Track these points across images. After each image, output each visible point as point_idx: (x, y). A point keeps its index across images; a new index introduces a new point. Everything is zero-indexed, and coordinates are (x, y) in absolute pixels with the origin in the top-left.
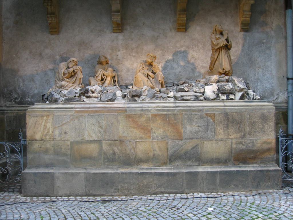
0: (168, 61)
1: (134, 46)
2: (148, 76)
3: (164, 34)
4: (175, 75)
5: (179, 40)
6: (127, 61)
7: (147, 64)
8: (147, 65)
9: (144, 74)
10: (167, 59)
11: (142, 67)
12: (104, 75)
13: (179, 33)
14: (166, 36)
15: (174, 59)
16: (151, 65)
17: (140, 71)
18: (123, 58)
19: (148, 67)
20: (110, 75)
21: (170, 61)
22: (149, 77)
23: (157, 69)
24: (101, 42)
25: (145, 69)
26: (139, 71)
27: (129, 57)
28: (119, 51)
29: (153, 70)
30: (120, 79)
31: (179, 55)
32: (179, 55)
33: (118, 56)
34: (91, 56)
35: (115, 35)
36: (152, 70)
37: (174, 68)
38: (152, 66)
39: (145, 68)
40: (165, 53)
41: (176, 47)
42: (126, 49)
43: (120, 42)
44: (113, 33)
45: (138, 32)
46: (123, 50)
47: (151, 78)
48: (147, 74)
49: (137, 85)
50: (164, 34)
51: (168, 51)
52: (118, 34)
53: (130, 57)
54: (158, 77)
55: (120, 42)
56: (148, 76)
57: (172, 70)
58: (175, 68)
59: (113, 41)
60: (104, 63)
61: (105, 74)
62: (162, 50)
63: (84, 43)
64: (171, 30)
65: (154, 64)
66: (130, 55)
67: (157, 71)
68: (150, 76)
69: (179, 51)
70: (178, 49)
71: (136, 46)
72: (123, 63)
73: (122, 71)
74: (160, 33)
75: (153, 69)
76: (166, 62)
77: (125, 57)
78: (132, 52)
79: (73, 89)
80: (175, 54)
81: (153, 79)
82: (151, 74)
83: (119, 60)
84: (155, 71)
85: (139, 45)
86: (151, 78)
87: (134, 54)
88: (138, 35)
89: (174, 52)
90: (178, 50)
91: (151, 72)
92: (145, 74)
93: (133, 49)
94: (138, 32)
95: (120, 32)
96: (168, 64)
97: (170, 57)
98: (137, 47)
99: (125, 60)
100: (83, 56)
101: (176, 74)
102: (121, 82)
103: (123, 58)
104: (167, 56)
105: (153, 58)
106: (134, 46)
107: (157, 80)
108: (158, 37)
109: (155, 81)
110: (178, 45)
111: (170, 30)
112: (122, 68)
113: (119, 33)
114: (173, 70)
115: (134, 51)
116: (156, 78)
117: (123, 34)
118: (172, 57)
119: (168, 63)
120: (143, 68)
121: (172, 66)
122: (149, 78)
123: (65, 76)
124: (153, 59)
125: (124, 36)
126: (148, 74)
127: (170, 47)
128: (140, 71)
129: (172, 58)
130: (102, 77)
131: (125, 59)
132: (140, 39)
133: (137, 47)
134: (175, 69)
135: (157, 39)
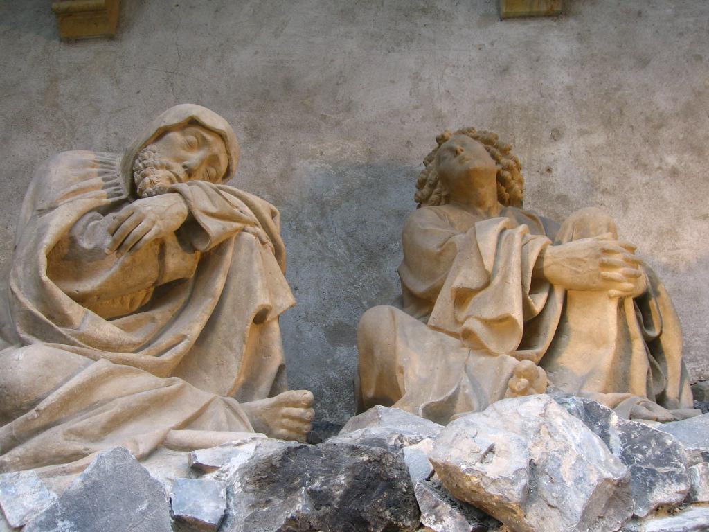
12: (539, 281)
18: (592, 186)
20: (616, 274)
24: (416, 77)
27: (638, 177)
28: (556, 135)
33: (549, 170)
34: (340, 175)
35: (516, 31)
42: (608, 124)
44: (504, 18)
45: (677, 15)
46: (582, 133)
52: (533, 24)
53: (646, 179)
55: (560, 78)
59: (505, 70)
60: (488, 191)
61: (550, 269)
63: (288, 85)
66: (640, 164)
71: (675, 100)
77: (609, 181)
78: (653, 143)
79: (163, 445)
87: (671, 160)
88: (681, 34)
93: (657, 123)
95: (550, 15)
100: (285, 175)
103: (592, 186)
106: (663, 101)
113: (547, 22)
115: (665, 134)
117: (572, 22)
123: (88, 286)
125: (581, 38)
130: (526, 307)
131: (605, 192)
132: (699, 58)
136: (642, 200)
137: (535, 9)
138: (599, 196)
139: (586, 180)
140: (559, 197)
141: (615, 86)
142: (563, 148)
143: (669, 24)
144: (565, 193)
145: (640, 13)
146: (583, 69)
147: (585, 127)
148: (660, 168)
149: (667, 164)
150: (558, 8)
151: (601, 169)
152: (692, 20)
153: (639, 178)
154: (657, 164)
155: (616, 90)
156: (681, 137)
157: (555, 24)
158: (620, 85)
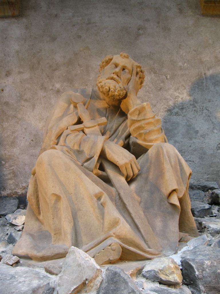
0: (176, 110)
1: (59, 58)
2: (102, 168)
3: (158, 23)
4: (201, 158)
5: (210, 42)
6: (34, 106)
7: (101, 105)
8: (98, 110)
9: (79, 152)
10: (171, 103)
11: (76, 120)
13: (206, 21)
14: (166, 29)
15: (195, 101)
16: (117, 108)
17: (59, 137)
18: (21, 98)
19: (104, 119)
21: (182, 109)
22: (111, 172)
23: (152, 128)
25: (86, 131)
26: (53, 138)
27: (42, 94)
28: (8, 74)
29: (129, 136)
30: (5, 173)
31: (212, 88)
32: (212, 88)
33: (3, 90)
36: (125, 134)
37: (197, 132)
38: (123, 115)
39: (87, 122)
40: (163, 82)
41: (201, 62)
42: (32, 68)
43: (15, 46)
45: (73, 16)
46: (20, 73)
47: (119, 180)
48: (96, 158)
49: (41, 217)
50: (158, 23)
51: (173, 77)
52: (7, 21)
53: (45, 94)
54: (161, 174)
55: (15, 46)
56: (102, 168)
57: (191, 139)
58: (200, 132)
62: (155, 73)
64: (181, 11)
65: (133, 104)
66: (43, 88)
67: (153, 137)
68: (116, 167)
69: (212, 77)
70: (208, 70)
72: (19, 116)
73: (13, 144)
74: (148, 20)
75: (131, 129)
76: (169, 111)
77: (28, 96)
80: (200, 85)
81: (133, 186)
82: (120, 156)
83: (7, 104)
84: (140, 142)
85: (76, 54)
86: (119, 180)
87: (58, 86)
88: (74, 25)
89: (194, 80)
90: (209, 73)
91: (121, 142)
92: (87, 154)
94: (73, 16)
95: (13, 17)
96: (174, 118)
97: (183, 96)
98: (70, 63)
99: (26, 104)
101: (205, 153)
102: (11, 182)
103: (21, 98)
104: (170, 92)
105: (129, 76)
106: (59, 58)
107: (156, 188)
108: (141, 32)
109: (145, 195)
110: (207, 57)
111: (180, 9)
112: (13, 132)
113: (13, 20)
114: (194, 140)
115: (57, 73)
116: (147, 179)
117: (24, 20)
118: (190, 95)
119: (177, 114)
120: (79, 122)
121: (189, 127)
122: (107, 180)
124: (129, 80)
125: (27, 28)
126: (103, 156)
127: (180, 64)
128: (59, 137)
129: (188, 98)
131: (26, 100)
132: (80, 37)
133: (70, 63)
134: (203, 136)
135: (138, 35)
136: (41, 104)
137: (6, 14)
138: (23, 102)
139: (18, 95)
140: (5, 103)
141: (39, 51)
142: (10, 79)
143: (69, 21)
144: (8, 101)
145: (56, 15)
146: (25, 42)
147: (22, 70)
148: (52, 89)
149: (55, 88)
150: (16, 13)
151: (25, 90)
152: (80, 18)
153: (42, 94)
154: (51, 88)
155: (38, 52)
156: (64, 75)
157: (16, 21)
158: (41, 50)
